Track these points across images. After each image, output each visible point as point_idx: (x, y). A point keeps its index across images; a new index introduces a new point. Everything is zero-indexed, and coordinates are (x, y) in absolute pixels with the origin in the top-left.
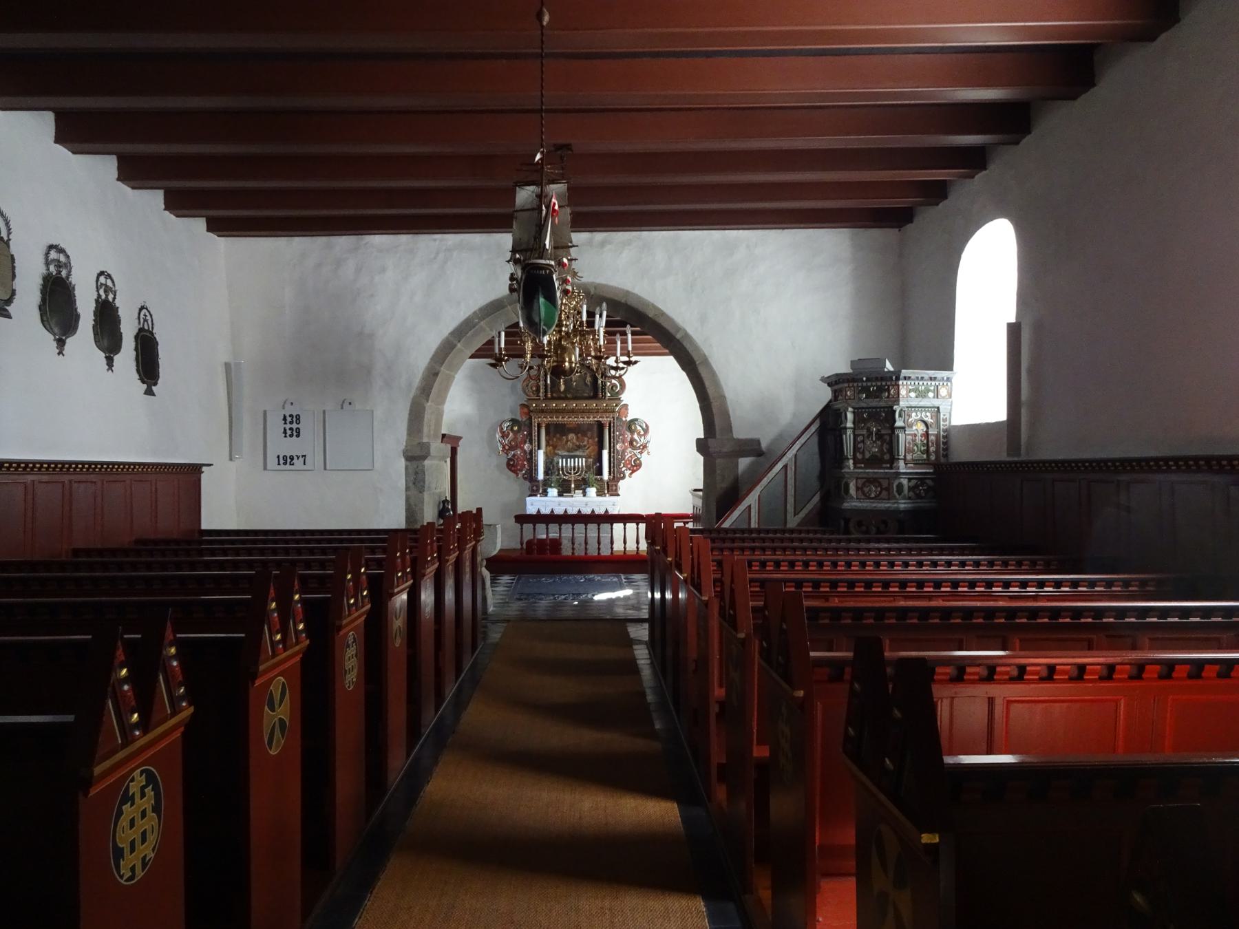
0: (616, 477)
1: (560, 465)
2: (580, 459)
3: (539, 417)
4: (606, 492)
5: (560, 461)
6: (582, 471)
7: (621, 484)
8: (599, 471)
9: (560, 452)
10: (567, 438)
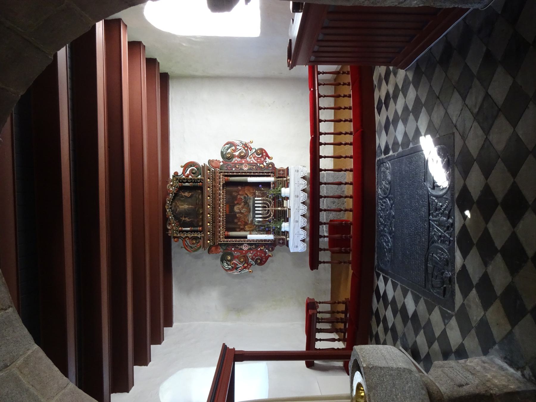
0: (272, 170)
1: (261, 219)
2: (256, 202)
3: (220, 238)
4: (285, 179)
5: (257, 219)
6: (267, 200)
7: (278, 166)
8: (267, 185)
9: (250, 219)
10: (238, 213)
